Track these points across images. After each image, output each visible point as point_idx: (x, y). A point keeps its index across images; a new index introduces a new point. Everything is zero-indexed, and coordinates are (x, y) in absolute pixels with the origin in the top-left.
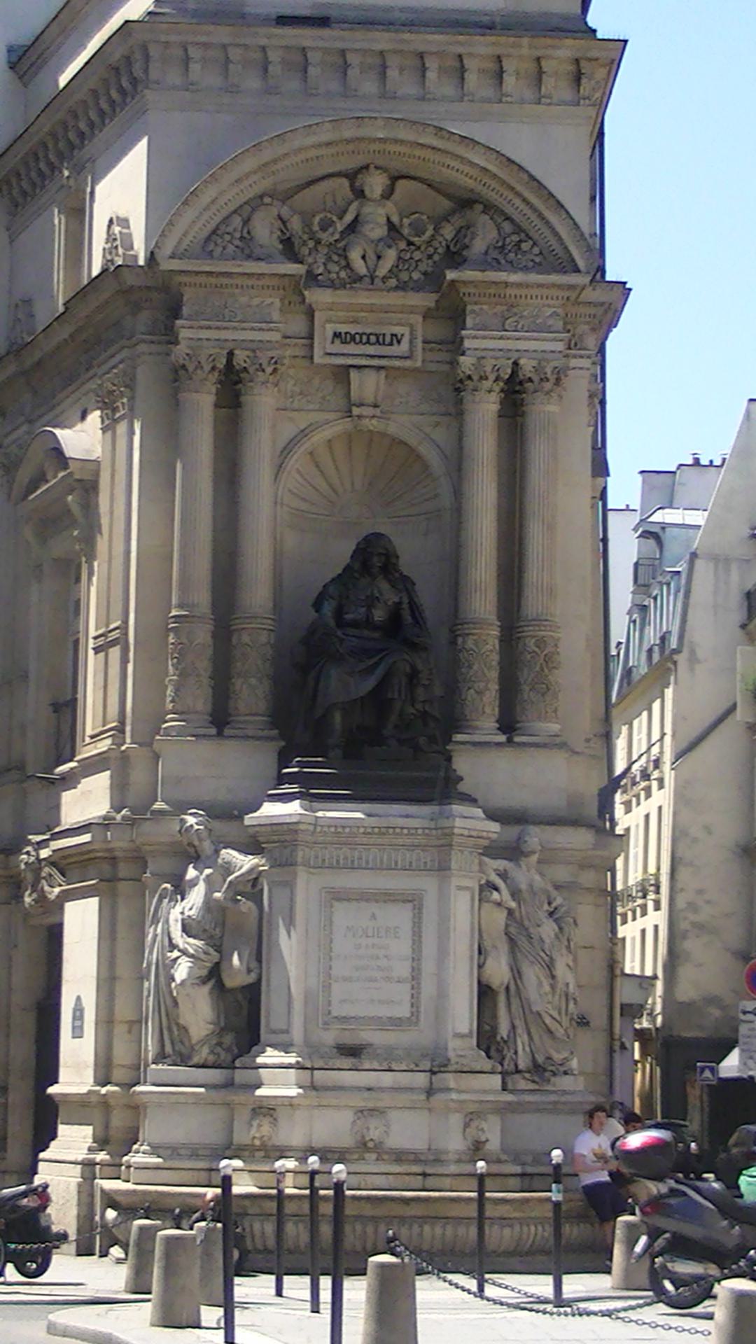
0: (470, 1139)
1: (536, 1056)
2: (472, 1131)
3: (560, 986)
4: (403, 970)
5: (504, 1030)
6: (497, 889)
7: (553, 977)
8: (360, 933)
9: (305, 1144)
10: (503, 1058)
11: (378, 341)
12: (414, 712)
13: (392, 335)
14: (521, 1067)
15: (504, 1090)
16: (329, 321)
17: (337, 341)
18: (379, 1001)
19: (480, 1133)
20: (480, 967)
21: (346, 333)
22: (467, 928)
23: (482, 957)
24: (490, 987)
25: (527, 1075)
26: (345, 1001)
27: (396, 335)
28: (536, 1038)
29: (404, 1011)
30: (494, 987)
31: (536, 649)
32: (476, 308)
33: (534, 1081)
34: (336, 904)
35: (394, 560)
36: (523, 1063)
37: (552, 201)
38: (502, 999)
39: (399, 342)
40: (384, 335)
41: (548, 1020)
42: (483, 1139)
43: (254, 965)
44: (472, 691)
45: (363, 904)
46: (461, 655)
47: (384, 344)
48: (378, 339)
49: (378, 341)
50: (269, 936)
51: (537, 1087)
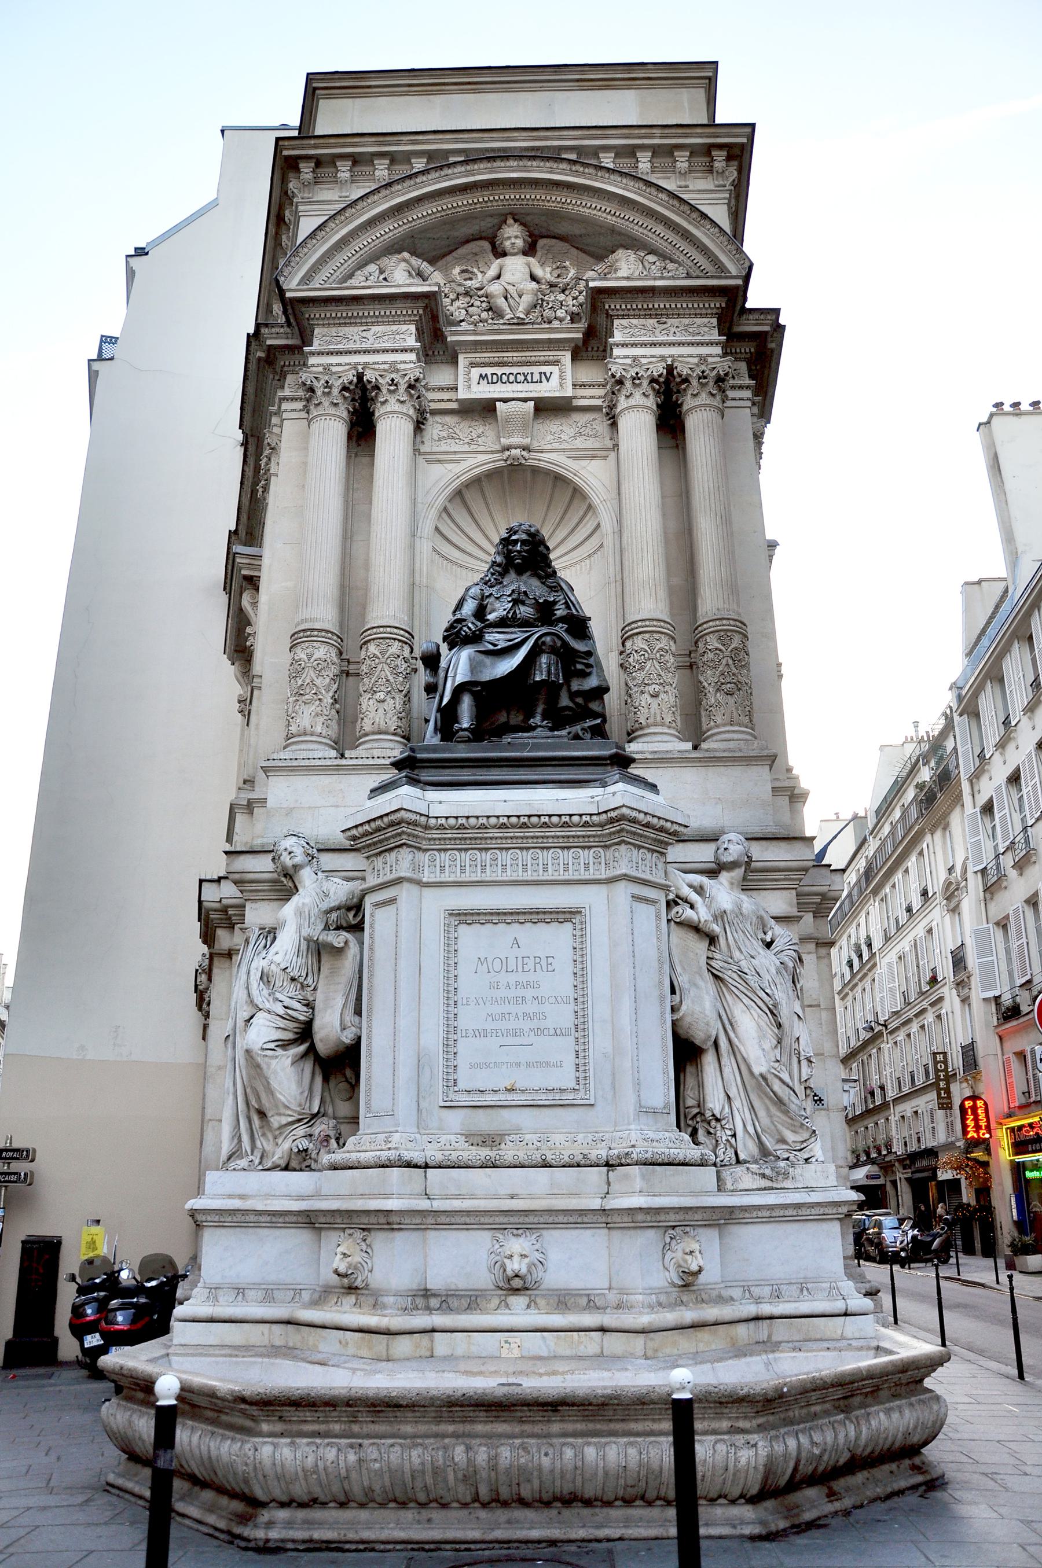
0: (672, 1268)
1: (763, 1138)
2: (677, 1254)
3: (786, 1042)
4: (563, 1016)
5: (715, 1103)
6: (692, 907)
7: (779, 1026)
8: (497, 967)
9: (415, 1287)
10: (717, 1146)
12: (571, 705)
13: (540, 373)
14: (742, 1156)
15: (719, 1190)
16: (473, 365)
17: (484, 382)
18: (528, 1065)
19: (689, 1258)
20: (673, 1009)
21: (492, 374)
22: (653, 953)
23: (677, 998)
24: (693, 1044)
25: (754, 1167)
26: (479, 1066)
28: (762, 1113)
29: (565, 1078)
30: (697, 1042)
31: (720, 647)
32: (625, 322)
33: (763, 1176)
34: (462, 928)
35: (542, 548)
36: (747, 1148)
37: (695, 215)
38: (709, 1060)
41: (777, 1086)
42: (694, 1268)
43: (350, 1017)
44: (646, 695)
45: (502, 926)
46: (631, 660)
48: (525, 377)
50: (371, 975)
51: (769, 1184)
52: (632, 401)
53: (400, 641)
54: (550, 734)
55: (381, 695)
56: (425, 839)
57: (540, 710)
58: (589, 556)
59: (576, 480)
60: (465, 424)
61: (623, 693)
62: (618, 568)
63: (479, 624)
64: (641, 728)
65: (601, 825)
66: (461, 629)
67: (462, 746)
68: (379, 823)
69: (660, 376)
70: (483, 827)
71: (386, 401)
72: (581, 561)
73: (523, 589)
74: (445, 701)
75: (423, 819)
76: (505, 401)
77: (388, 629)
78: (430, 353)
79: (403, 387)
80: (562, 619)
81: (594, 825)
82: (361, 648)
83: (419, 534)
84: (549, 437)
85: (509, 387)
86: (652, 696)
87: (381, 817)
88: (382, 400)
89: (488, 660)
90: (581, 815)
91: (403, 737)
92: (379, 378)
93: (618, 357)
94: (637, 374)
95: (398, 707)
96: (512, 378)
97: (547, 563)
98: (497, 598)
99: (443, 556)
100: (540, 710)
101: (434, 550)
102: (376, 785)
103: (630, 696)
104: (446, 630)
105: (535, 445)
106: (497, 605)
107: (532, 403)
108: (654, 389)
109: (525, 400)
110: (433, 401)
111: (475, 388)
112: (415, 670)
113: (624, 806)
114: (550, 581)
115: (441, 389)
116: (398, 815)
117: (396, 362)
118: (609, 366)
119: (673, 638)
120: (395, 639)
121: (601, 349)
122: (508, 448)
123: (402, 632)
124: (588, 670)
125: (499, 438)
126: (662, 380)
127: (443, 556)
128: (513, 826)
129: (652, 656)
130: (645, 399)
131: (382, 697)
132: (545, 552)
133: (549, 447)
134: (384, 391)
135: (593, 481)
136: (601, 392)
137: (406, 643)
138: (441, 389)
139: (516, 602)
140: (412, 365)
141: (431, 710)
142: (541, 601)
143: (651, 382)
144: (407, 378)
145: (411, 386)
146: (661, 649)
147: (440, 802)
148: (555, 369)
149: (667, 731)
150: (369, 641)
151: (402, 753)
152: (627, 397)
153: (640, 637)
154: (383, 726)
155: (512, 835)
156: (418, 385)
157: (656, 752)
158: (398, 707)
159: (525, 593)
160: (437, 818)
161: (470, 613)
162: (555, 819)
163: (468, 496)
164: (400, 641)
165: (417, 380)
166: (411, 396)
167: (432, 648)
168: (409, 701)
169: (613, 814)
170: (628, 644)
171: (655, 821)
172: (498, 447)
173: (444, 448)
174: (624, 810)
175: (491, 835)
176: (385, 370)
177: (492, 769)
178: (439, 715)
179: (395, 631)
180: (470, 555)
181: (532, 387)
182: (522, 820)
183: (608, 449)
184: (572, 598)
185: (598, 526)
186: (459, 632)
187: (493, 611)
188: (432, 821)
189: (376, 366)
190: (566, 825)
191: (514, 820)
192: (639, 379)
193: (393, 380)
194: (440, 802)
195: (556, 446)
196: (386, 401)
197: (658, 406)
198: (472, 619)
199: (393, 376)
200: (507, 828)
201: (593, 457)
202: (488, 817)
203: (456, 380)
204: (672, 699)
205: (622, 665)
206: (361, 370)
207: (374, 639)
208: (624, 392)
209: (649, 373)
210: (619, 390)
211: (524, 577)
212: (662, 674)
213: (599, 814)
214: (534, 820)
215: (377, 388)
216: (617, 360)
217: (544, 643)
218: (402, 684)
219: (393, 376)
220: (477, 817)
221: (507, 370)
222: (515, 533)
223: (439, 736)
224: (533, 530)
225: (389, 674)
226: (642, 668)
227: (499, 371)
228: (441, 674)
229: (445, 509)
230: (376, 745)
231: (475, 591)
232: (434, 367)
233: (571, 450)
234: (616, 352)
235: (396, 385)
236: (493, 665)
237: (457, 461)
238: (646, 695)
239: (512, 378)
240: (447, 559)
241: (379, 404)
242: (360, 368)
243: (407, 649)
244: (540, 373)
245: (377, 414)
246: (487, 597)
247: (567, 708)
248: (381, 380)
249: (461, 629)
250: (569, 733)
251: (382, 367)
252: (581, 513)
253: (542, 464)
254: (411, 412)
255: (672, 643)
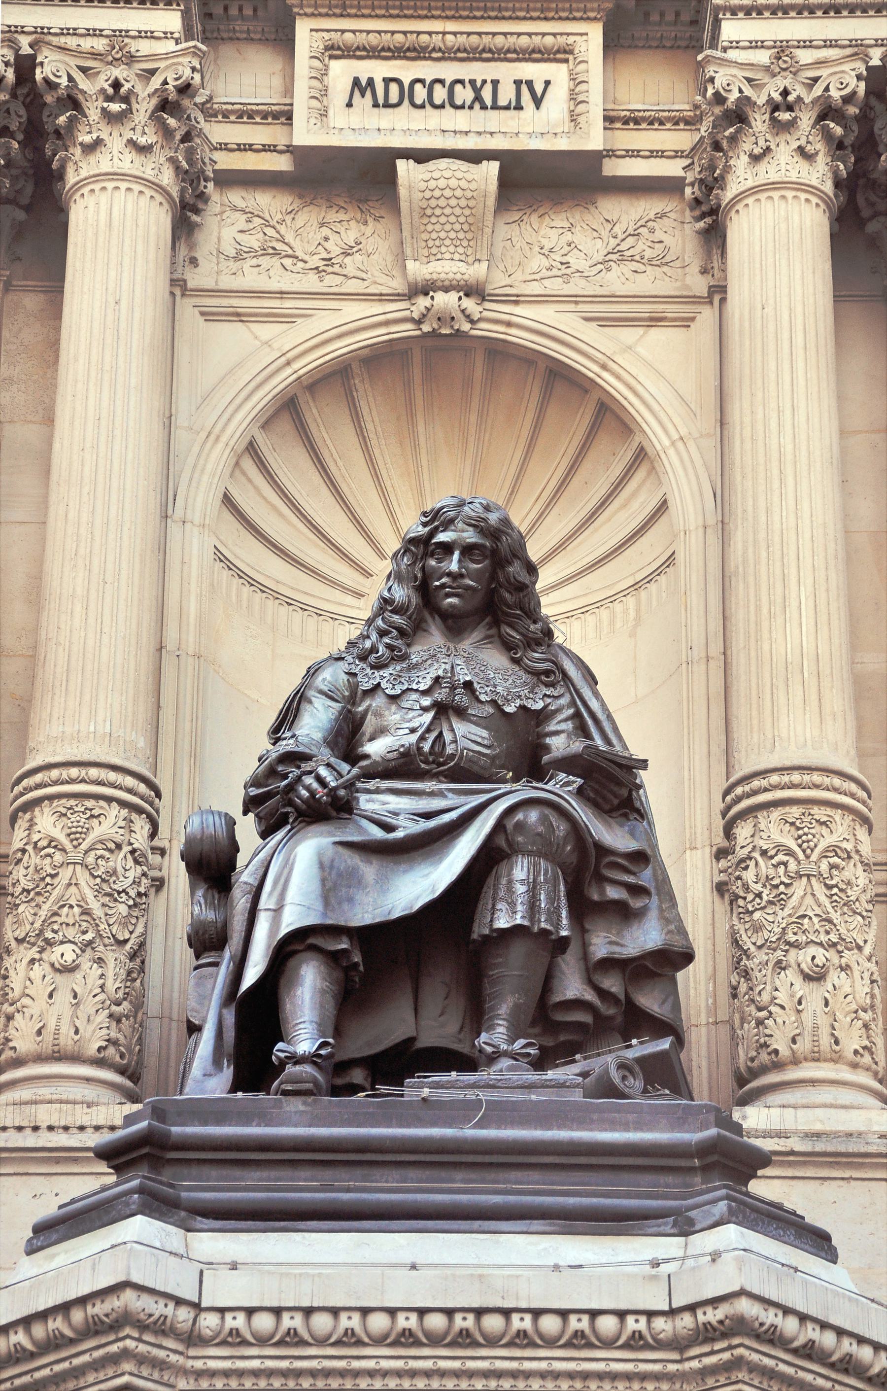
11: (478, 98)
12: (589, 996)
13: (518, 83)
17: (363, 103)
21: (387, 81)
27: (530, 84)
35: (515, 569)
39: (538, 102)
40: (495, 83)
44: (791, 975)
46: (749, 876)
47: (495, 107)
48: (477, 91)
49: (478, 98)
52: (768, 172)
53: (123, 804)
54: (533, 1076)
55: (69, 953)
56: (185, 1372)
57: (504, 1010)
58: (636, 586)
59: (608, 381)
60: (308, 217)
61: (723, 964)
62: (715, 624)
63: (344, 767)
64: (778, 1066)
65: (678, 1344)
66: (299, 779)
67: (296, 1105)
68: (57, 1324)
69: (848, 99)
70: (350, 1339)
71: (98, 143)
72: (612, 599)
73: (464, 675)
74: (251, 976)
75: (184, 1315)
76: (422, 156)
77: (94, 772)
78: (218, 10)
79: (144, 107)
80: (569, 764)
81: (660, 1345)
82: (13, 819)
83: (179, 513)
84: (537, 262)
85: (433, 119)
86: (807, 978)
87: (65, 1308)
88: (87, 139)
89: (369, 870)
90: (621, 1314)
91: (122, 1071)
92: (78, 76)
93: (735, 45)
94: (785, 93)
95: (111, 986)
96: (440, 93)
97: (532, 612)
98: (394, 698)
99: (241, 575)
100: (504, 1010)
101: (221, 557)
102: (49, 1209)
103: (746, 974)
104: (255, 782)
105: (498, 282)
106: (393, 716)
107: (492, 168)
108: (827, 135)
109: (474, 157)
110: (223, 147)
111: (338, 116)
112: (159, 884)
113: (742, 1293)
114: (536, 657)
115: (246, 115)
116: (114, 1304)
117: (124, 34)
118: (710, 71)
119: (865, 821)
120: (109, 799)
121: (686, 17)
122: (425, 289)
123: (130, 781)
124: (636, 903)
125: (401, 259)
126: (852, 110)
127: (241, 575)
128: (434, 1340)
129: (807, 867)
130: (803, 165)
131: (69, 957)
132: (524, 577)
133: (535, 288)
134: (93, 113)
135: (651, 385)
136: (683, 139)
137: (140, 811)
138: (246, 115)
139: (442, 710)
140: (170, 46)
141: (204, 999)
142: (510, 709)
143: (822, 117)
144: (156, 82)
145: (164, 106)
146: (834, 850)
147: (234, 1266)
148: (558, 73)
149: (846, 1074)
150: (38, 801)
151: (129, 1120)
152: (756, 159)
153: (776, 814)
154: (67, 1039)
155: (428, 1364)
156: (186, 102)
157: (817, 1135)
158: (111, 986)
159: (468, 685)
160: (222, 1311)
161: (318, 736)
162: (550, 1324)
163: (312, 413)
164: (123, 804)
165: (185, 89)
166: (167, 133)
167: (215, 827)
168: (142, 970)
169: (712, 1316)
170: (743, 832)
171: (828, 1340)
172: (398, 285)
173: (251, 279)
174: (745, 1307)
175: (370, 1364)
176: (95, 55)
177: (377, 1172)
178: (230, 1018)
179: (112, 776)
180: (313, 572)
181: (493, 120)
182: (460, 1322)
183: (694, 300)
184: (594, 705)
185: (663, 507)
186: (291, 788)
187: (381, 731)
188: (209, 1322)
189: (71, 42)
190: (580, 1340)
191: (436, 1322)
192: (790, 108)
193: (116, 85)
194: (234, 1266)
195: (555, 286)
196: (98, 143)
197: (838, 184)
198: (325, 754)
199: (118, 72)
200: (417, 1343)
201: (655, 321)
202: (365, 1312)
203: (289, 90)
204: (862, 989)
205: (721, 888)
206: (26, 50)
207: (51, 798)
208: (747, 145)
209: (818, 91)
210: (734, 140)
211: (467, 644)
212: (835, 916)
213: (672, 1312)
214: (493, 1323)
215: (72, 102)
216: (732, 54)
217: (520, 827)
218: (124, 922)
219: (118, 72)
220: (335, 1312)
221: (427, 70)
222: (448, 524)
223: (228, 1073)
224: (493, 518)
225: (89, 894)
226: (779, 901)
227: (406, 71)
228: (240, 901)
229: (252, 448)
230: (44, 1091)
231: (329, 676)
232: (227, 50)
233: (594, 299)
234: (730, 29)
235: (126, 99)
236: (383, 883)
237: (286, 318)
238: (791, 975)
239: (440, 93)
240: (252, 582)
241: (78, 151)
242: (24, 42)
243: (141, 827)
244: (518, 83)
245: (71, 178)
246: (368, 693)
247: (578, 1004)
248: (83, 83)
249: (299, 779)
250: (585, 1075)
251: (87, 44)
252: (617, 470)
253: (516, 336)
254: (167, 177)
255: (862, 833)
